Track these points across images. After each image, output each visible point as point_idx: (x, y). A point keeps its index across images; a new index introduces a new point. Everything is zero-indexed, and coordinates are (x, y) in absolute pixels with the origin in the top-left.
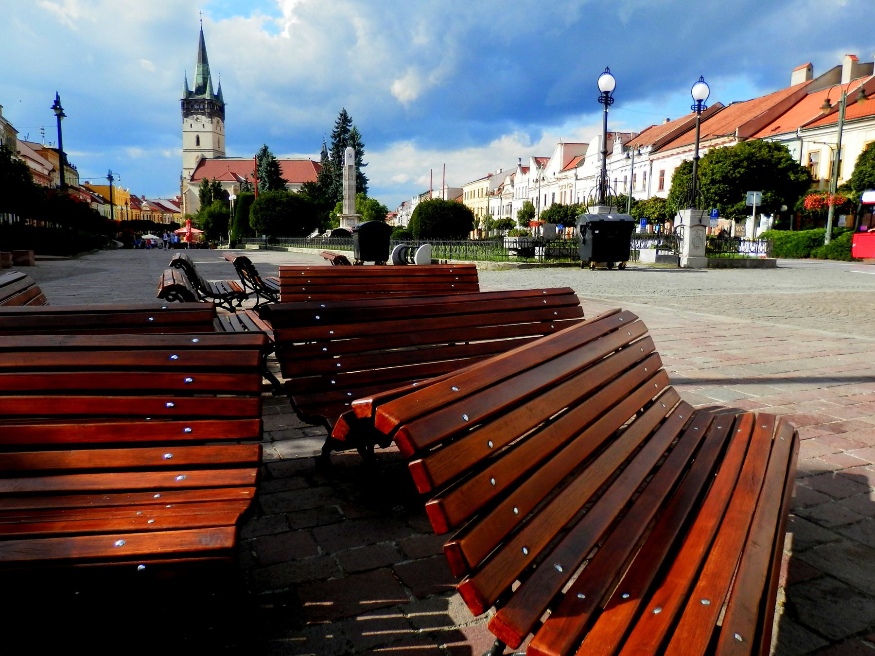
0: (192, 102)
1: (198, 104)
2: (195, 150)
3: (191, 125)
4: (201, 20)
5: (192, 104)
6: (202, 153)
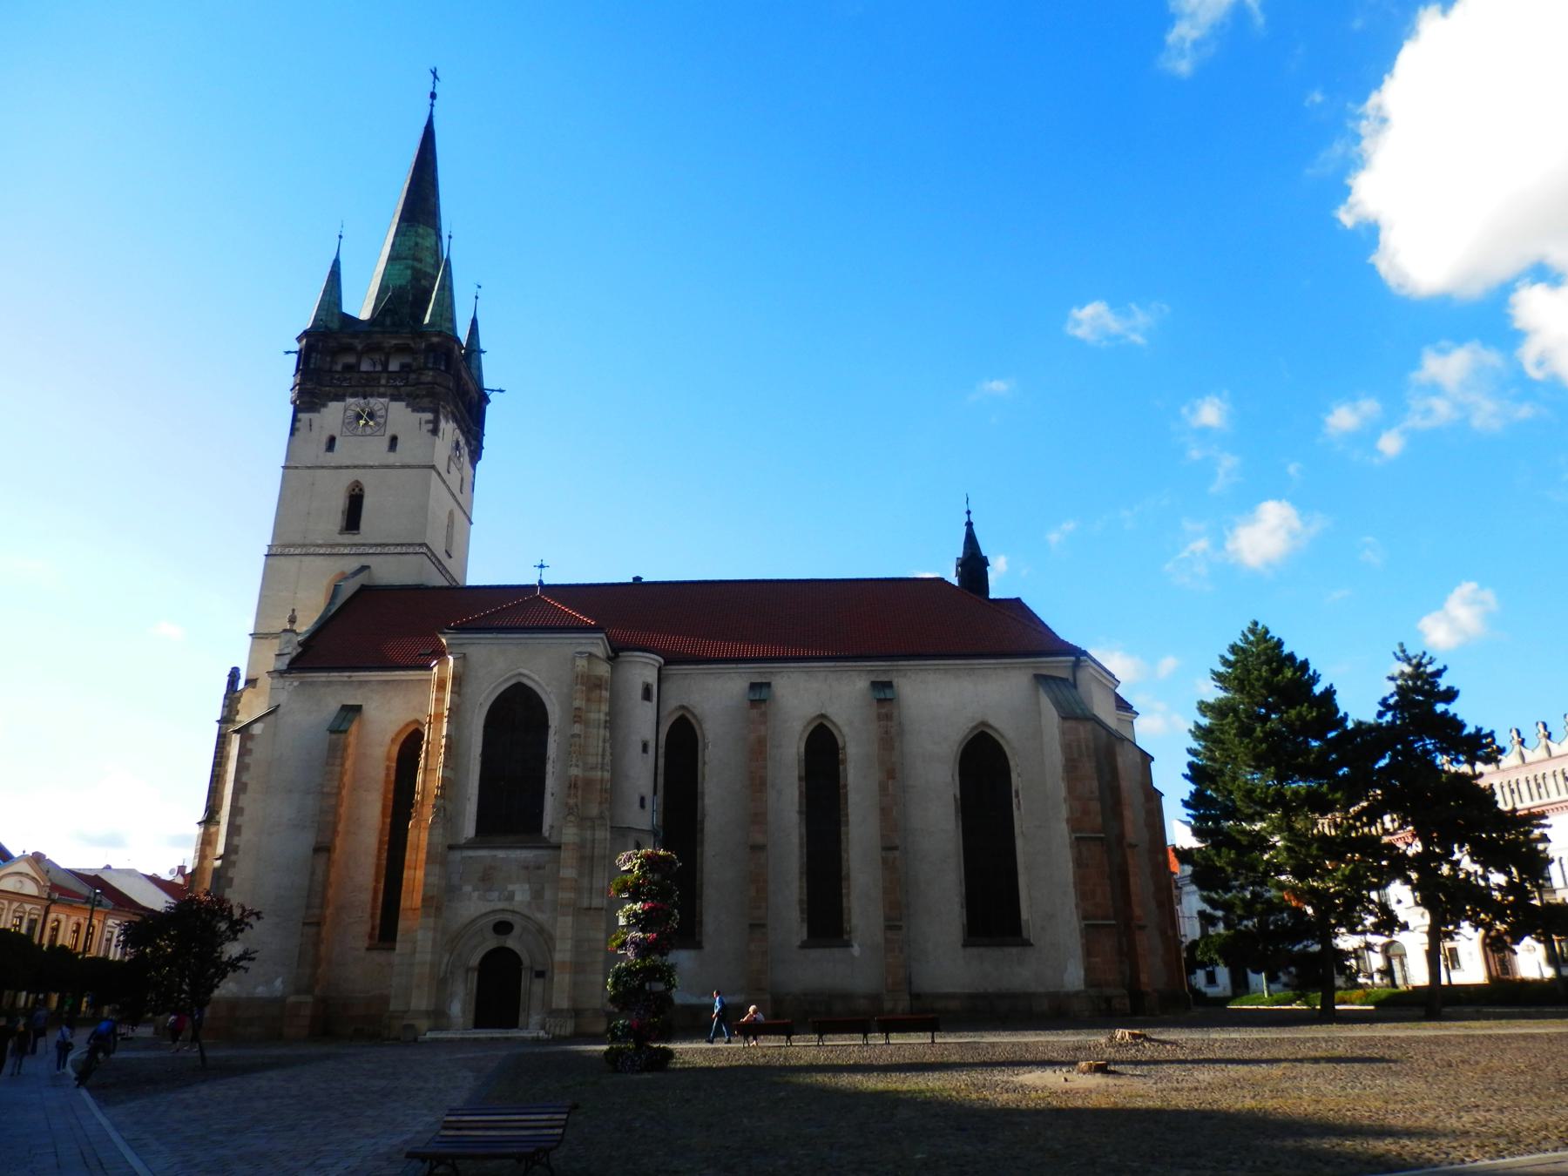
0: (349, 349)
1: (376, 357)
2: (330, 551)
3: (332, 440)
4: (433, 96)
5: (351, 359)
6: (364, 561)
